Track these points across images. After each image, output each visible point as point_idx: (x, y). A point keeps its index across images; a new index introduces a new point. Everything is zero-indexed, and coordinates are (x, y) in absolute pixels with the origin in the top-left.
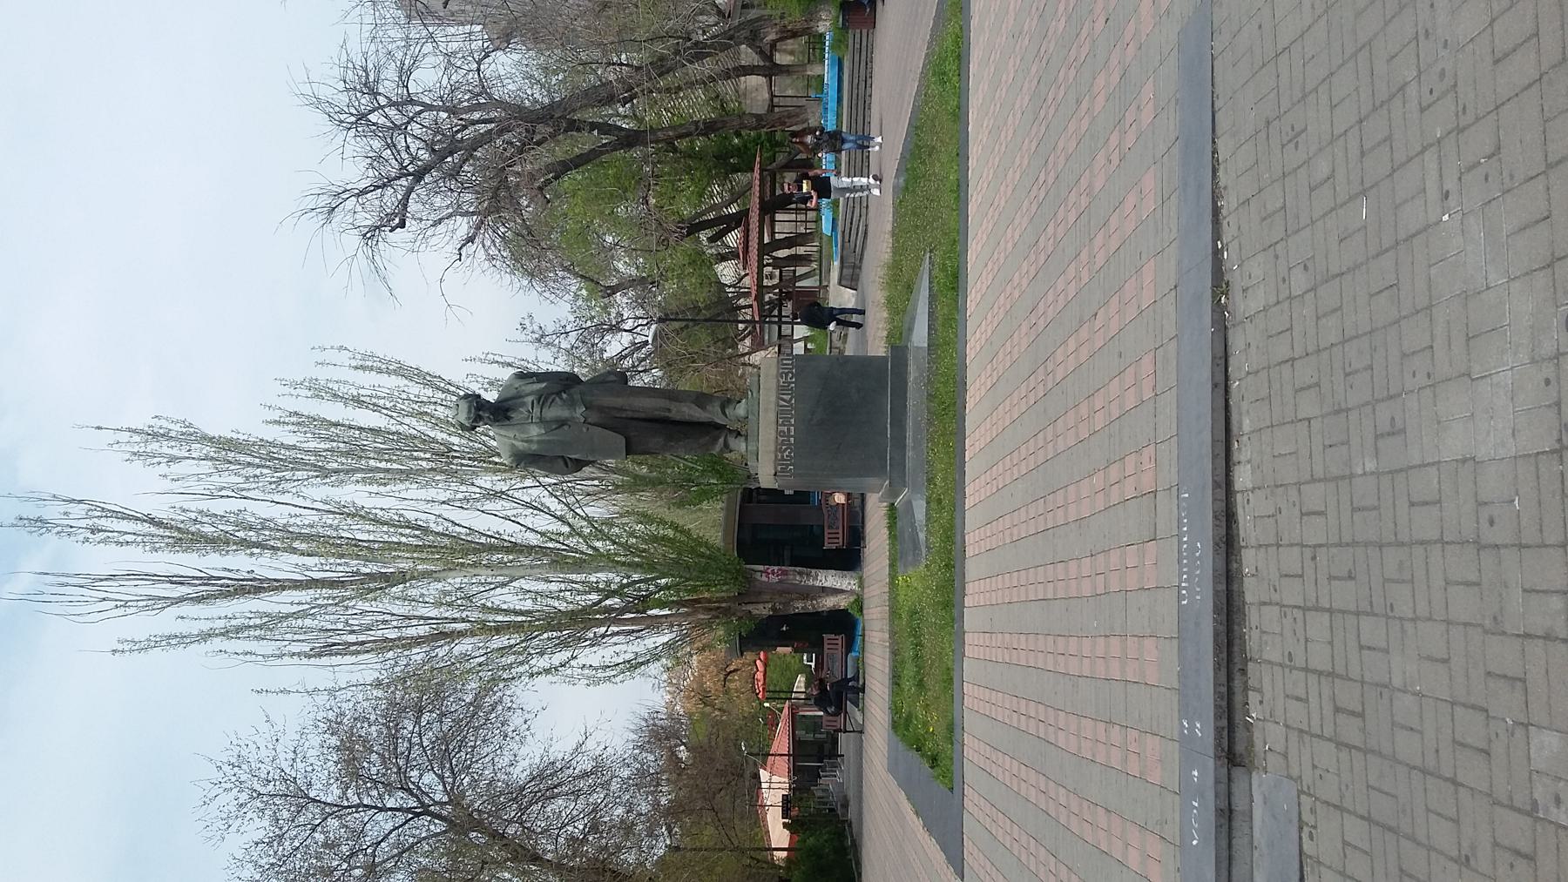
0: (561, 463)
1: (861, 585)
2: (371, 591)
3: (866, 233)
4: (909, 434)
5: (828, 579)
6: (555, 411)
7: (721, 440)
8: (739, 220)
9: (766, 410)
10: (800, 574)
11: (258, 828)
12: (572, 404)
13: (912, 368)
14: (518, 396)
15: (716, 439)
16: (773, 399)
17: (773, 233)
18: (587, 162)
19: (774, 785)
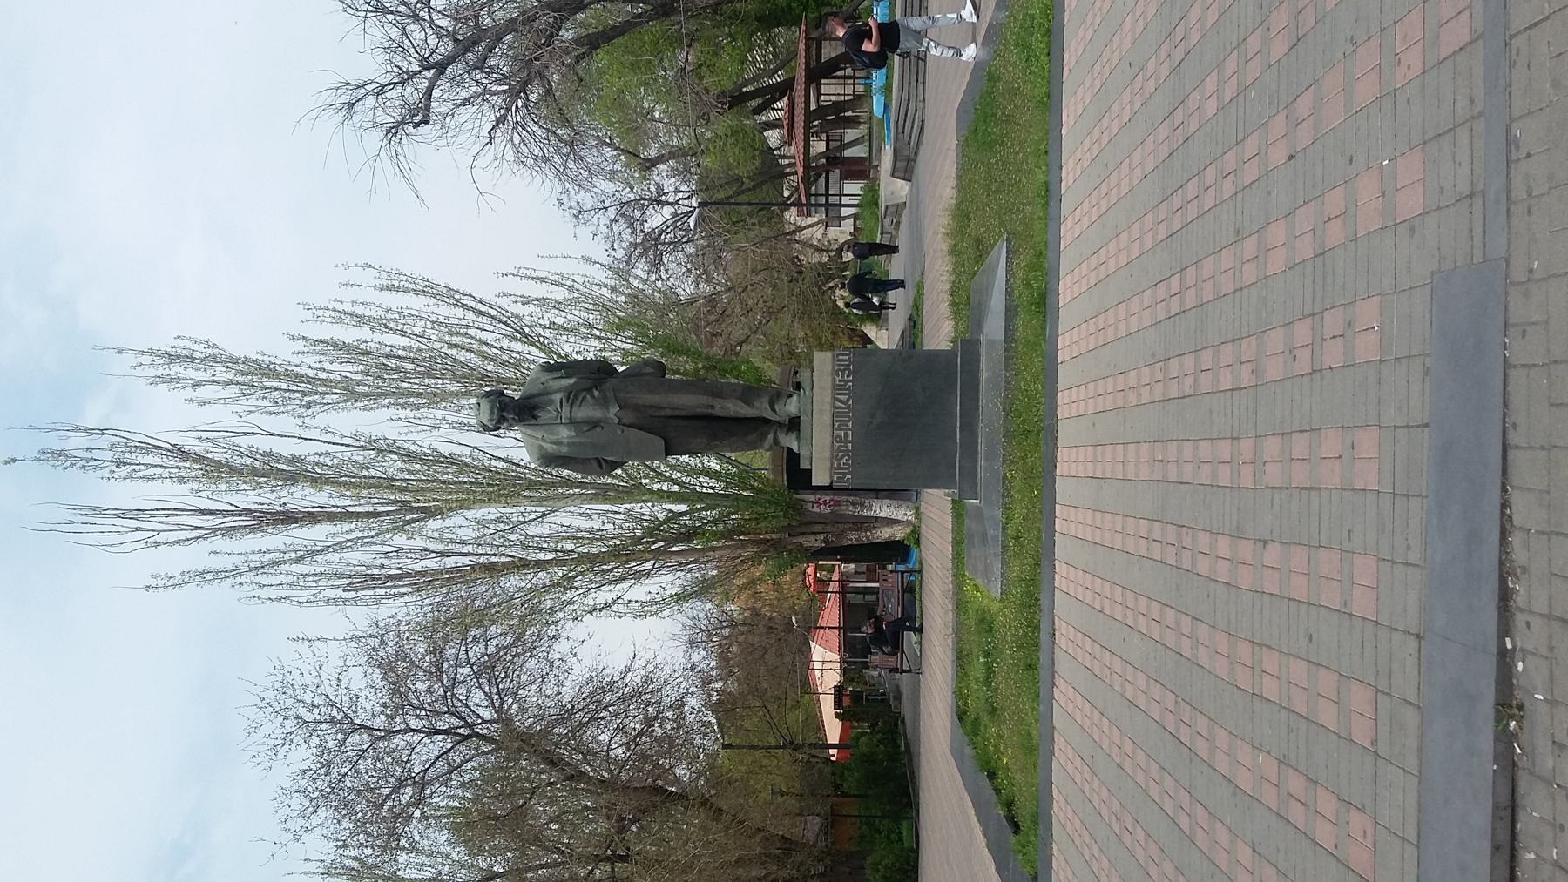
0: (595, 464)
1: (918, 515)
2: (408, 522)
3: (922, 128)
4: (981, 439)
5: (883, 509)
6: (585, 412)
7: (771, 437)
8: (786, 88)
10: (853, 504)
11: (302, 756)
12: (604, 403)
13: (984, 365)
14: (546, 393)
15: (764, 436)
16: (829, 399)
17: (819, 94)
18: (622, 33)
19: (825, 663)
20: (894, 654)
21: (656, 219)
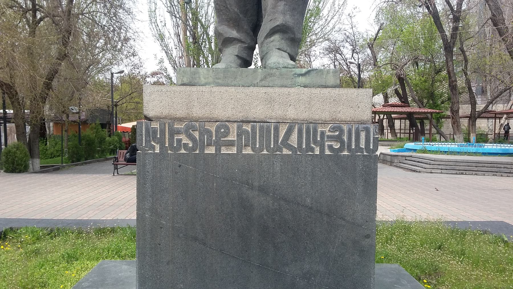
3: (414, 171)
7: (234, 34)
9: (270, 101)
15: (235, 23)
16: (292, 113)
20: (125, 160)
21: (347, 51)
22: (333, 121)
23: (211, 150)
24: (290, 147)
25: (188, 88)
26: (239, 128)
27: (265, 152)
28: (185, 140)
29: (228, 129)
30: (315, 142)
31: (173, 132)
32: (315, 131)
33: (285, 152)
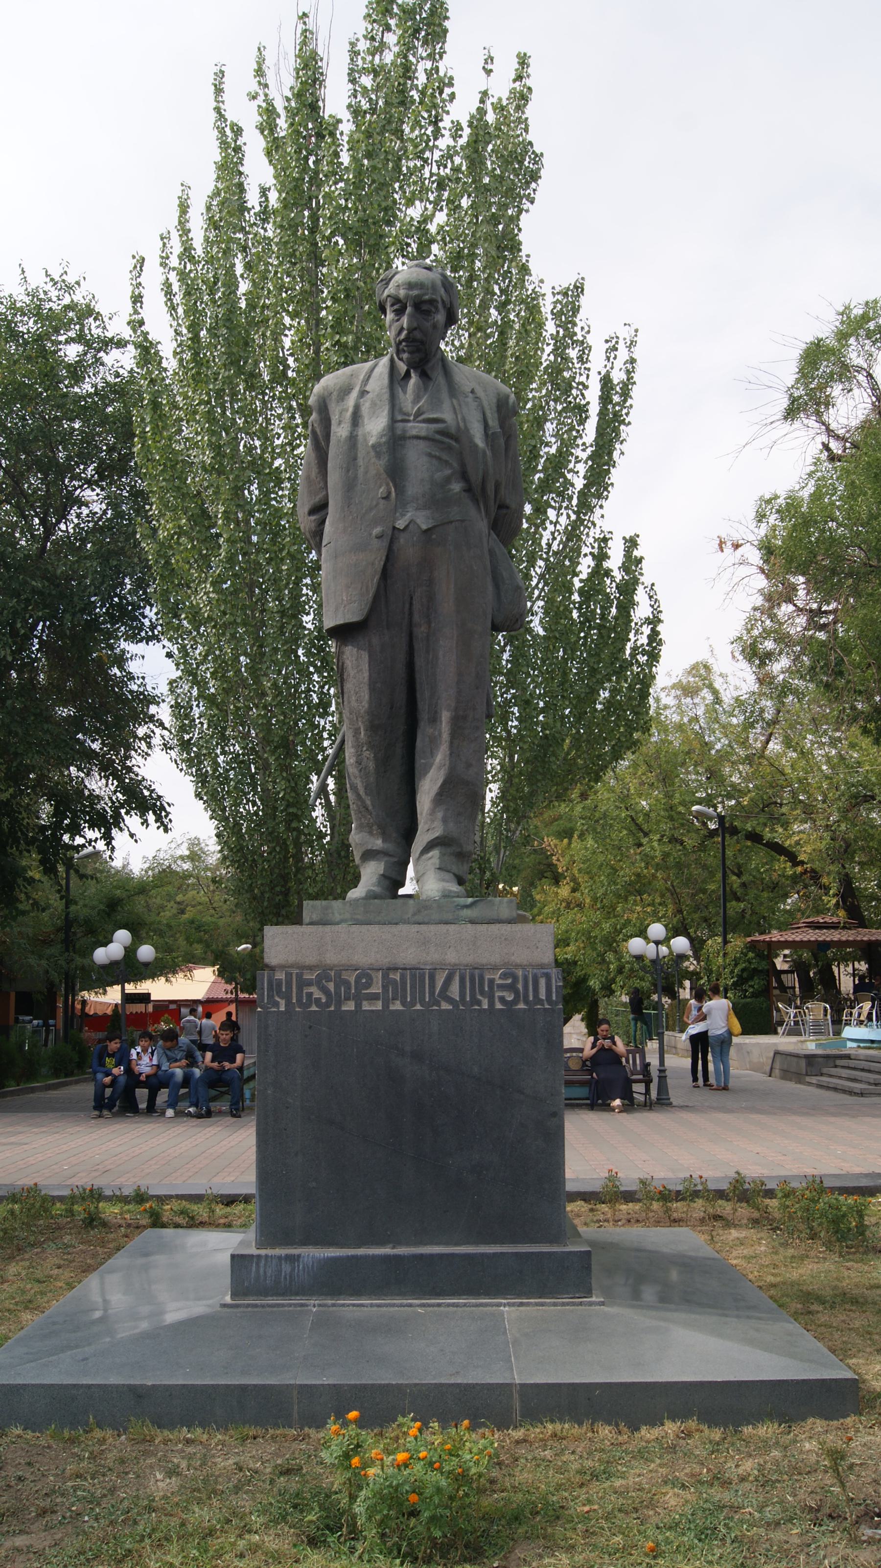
6: (418, 463)
7: (378, 843)
12: (436, 500)
16: (452, 957)
22: (505, 964)
23: (350, 1006)
24: (450, 1000)
25: (320, 928)
26: (385, 976)
27: (418, 1007)
28: (317, 994)
29: (370, 978)
30: (482, 993)
31: (303, 983)
32: (482, 978)
33: (445, 1006)
